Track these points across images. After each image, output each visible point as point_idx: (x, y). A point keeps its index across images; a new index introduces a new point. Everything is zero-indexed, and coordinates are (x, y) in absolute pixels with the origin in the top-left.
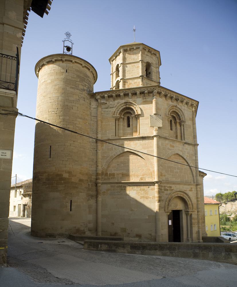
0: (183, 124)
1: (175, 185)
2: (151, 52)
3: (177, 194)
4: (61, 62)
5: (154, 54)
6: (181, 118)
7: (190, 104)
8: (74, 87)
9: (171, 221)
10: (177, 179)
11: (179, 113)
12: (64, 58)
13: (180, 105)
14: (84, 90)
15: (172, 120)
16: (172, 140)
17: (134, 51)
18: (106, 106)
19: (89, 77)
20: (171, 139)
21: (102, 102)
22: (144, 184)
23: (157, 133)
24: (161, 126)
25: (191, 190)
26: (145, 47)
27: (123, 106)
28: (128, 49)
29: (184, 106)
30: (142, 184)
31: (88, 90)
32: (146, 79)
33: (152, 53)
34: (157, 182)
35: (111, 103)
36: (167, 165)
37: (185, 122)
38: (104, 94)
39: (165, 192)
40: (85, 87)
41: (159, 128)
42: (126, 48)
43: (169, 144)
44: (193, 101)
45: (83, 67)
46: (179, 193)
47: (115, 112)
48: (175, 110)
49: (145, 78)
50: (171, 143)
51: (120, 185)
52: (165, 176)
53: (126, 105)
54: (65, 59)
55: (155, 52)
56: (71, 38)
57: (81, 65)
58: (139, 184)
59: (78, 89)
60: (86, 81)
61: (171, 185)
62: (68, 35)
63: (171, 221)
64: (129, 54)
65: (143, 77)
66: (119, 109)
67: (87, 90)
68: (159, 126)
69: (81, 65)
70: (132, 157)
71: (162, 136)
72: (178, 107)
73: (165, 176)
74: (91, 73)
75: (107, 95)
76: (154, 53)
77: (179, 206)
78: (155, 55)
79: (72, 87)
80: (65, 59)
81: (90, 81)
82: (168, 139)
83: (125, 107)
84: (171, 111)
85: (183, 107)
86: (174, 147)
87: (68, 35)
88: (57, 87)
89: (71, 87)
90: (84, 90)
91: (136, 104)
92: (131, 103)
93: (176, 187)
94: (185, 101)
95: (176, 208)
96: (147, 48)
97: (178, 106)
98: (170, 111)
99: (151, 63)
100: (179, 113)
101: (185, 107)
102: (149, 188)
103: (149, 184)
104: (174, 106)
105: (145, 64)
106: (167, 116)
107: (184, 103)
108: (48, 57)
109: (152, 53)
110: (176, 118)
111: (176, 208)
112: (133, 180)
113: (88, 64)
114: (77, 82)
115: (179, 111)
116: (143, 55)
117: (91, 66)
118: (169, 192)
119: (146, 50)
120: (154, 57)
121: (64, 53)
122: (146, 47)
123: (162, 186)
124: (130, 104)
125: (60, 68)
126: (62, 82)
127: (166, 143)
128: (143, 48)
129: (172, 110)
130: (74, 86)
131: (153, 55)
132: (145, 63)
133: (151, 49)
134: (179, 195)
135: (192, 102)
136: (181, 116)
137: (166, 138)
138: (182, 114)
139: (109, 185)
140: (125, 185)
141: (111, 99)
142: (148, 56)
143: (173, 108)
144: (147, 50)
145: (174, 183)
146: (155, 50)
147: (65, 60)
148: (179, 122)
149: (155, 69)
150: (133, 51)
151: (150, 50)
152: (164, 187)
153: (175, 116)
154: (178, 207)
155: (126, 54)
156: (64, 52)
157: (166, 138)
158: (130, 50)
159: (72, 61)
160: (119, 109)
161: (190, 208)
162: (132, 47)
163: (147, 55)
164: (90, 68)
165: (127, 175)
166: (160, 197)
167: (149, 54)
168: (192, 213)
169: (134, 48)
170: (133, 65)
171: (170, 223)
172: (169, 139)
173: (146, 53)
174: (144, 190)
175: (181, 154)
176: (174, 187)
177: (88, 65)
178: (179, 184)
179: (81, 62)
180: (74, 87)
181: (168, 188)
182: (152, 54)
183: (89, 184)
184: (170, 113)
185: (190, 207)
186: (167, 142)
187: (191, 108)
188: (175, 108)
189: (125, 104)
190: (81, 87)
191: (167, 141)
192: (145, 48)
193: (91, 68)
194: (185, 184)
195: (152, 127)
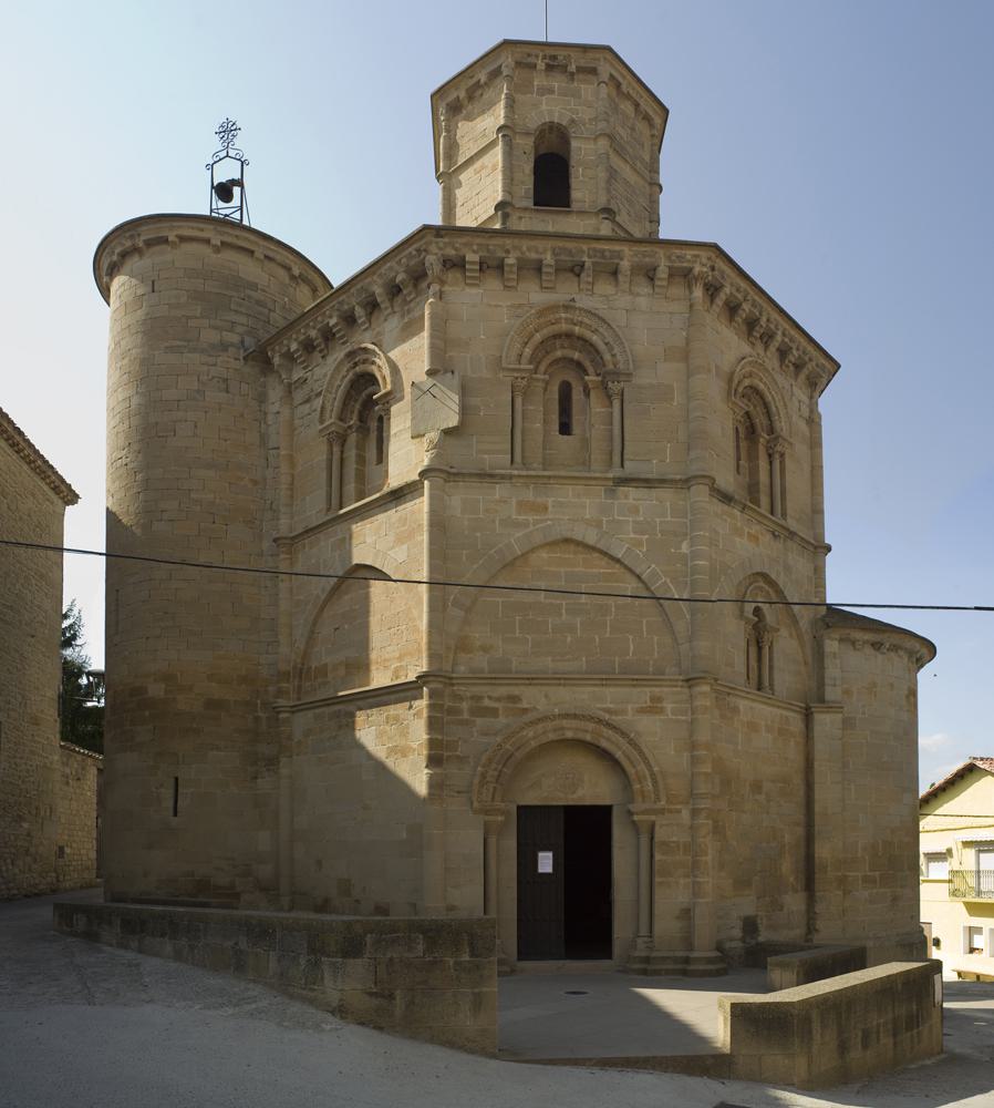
0: (614, 387)
1: (545, 688)
2: (563, 69)
3: (555, 730)
4: (136, 258)
5: (581, 70)
6: (607, 357)
7: (662, 273)
8: (178, 343)
9: (550, 854)
10: (569, 660)
11: (595, 338)
12: (139, 235)
13: (599, 298)
14: (224, 347)
15: (574, 384)
16: (527, 476)
17: (484, 97)
18: (306, 389)
19: (254, 287)
20: (519, 476)
21: (295, 377)
22: (397, 696)
23: (431, 460)
24: (453, 421)
25: (654, 708)
26: (529, 55)
27: (348, 371)
28: (462, 94)
29: (631, 293)
30: (393, 697)
31: (249, 341)
32: (527, 215)
33: (573, 68)
34: (423, 679)
35: (318, 371)
36: (500, 600)
37: (630, 375)
38: (285, 342)
39: (479, 721)
40: (231, 331)
41: (447, 432)
42: (455, 96)
43: (514, 500)
44: (678, 252)
45: (217, 250)
46: (565, 723)
47: (323, 408)
48: (564, 327)
49: (526, 209)
50: (529, 495)
51: (336, 708)
52: (485, 649)
53: (356, 364)
54: (142, 238)
55: (590, 55)
56: (239, 142)
57: (207, 241)
58: (385, 698)
59: (194, 350)
60: (232, 307)
61: (515, 691)
62: (228, 131)
63: (550, 854)
64: (469, 118)
65: (508, 210)
66: (337, 391)
67: (242, 342)
68: (444, 426)
69: (207, 241)
70: (377, 588)
71: (464, 471)
72: (580, 309)
73: (485, 649)
74: (271, 265)
75: (296, 340)
76: (582, 63)
77: (593, 788)
78: (593, 71)
79: (172, 347)
80: (142, 238)
81: (258, 303)
82: (503, 477)
83: (351, 375)
84: (538, 337)
85: (623, 301)
86: (546, 508)
87: (228, 131)
88: (126, 361)
89: (167, 347)
90: (224, 347)
91: (377, 349)
92: (365, 349)
93: (546, 696)
94: (625, 265)
95: (575, 796)
96: (537, 56)
97: (584, 301)
98: (531, 336)
99: (564, 123)
100: (588, 334)
101: (638, 295)
102: (412, 711)
103: (409, 694)
104: (553, 308)
105: (526, 144)
106: (504, 369)
107: (621, 278)
108: (104, 250)
109: (573, 68)
110: (587, 364)
111: (575, 796)
112: (380, 679)
113: (238, 232)
114: (191, 323)
115: (588, 327)
116: (519, 97)
117: (252, 237)
118: (502, 720)
119: (535, 66)
120: (587, 89)
121: (213, 214)
122: (527, 49)
123: (458, 698)
124: (365, 356)
125: (133, 280)
126: (140, 336)
127: (497, 497)
128: (516, 63)
129: (546, 332)
130: (180, 340)
131: (581, 76)
132: (528, 134)
133: (561, 54)
134: (569, 735)
135: (669, 258)
136: (601, 347)
137: (492, 476)
138: (609, 339)
139: (310, 714)
140: (350, 707)
141: (317, 355)
142: (551, 91)
143: (551, 317)
144: (541, 65)
145: (531, 680)
146: (585, 48)
147: (144, 241)
148: (602, 381)
149: (592, 146)
150: (482, 95)
151: (554, 58)
152: (472, 698)
153: (576, 356)
154: (580, 792)
155: (459, 125)
156: (211, 211)
157: (487, 476)
158: (471, 98)
159: (165, 241)
160: (337, 391)
161: (644, 797)
162: (475, 80)
163: (544, 91)
164: (252, 248)
165: (361, 666)
166: (432, 744)
167: (557, 82)
168: (653, 818)
169: (482, 81)
170: (478, 165)
171: (546, 863)
172: (511, 477)
173: (539, 80)
174: (397, 719)
175: (591, 537)
176: (533, 698)
177: (237, 236)
178: (561, 679)
179: (202, 230)
180: (178, 343)
181: (496, 705)
182: (572, 74)
183: (257, 719)
184: (528, 351)
185: (642, 792)
186: (499, 491)
187: (678, 290)
188: (563, 315)
189: (351, 364)
190: (210, 336)
191: (498, 486)
192: (529, 60)
193: (256, 243)
194: (606, 681)
195: (417, 436)
